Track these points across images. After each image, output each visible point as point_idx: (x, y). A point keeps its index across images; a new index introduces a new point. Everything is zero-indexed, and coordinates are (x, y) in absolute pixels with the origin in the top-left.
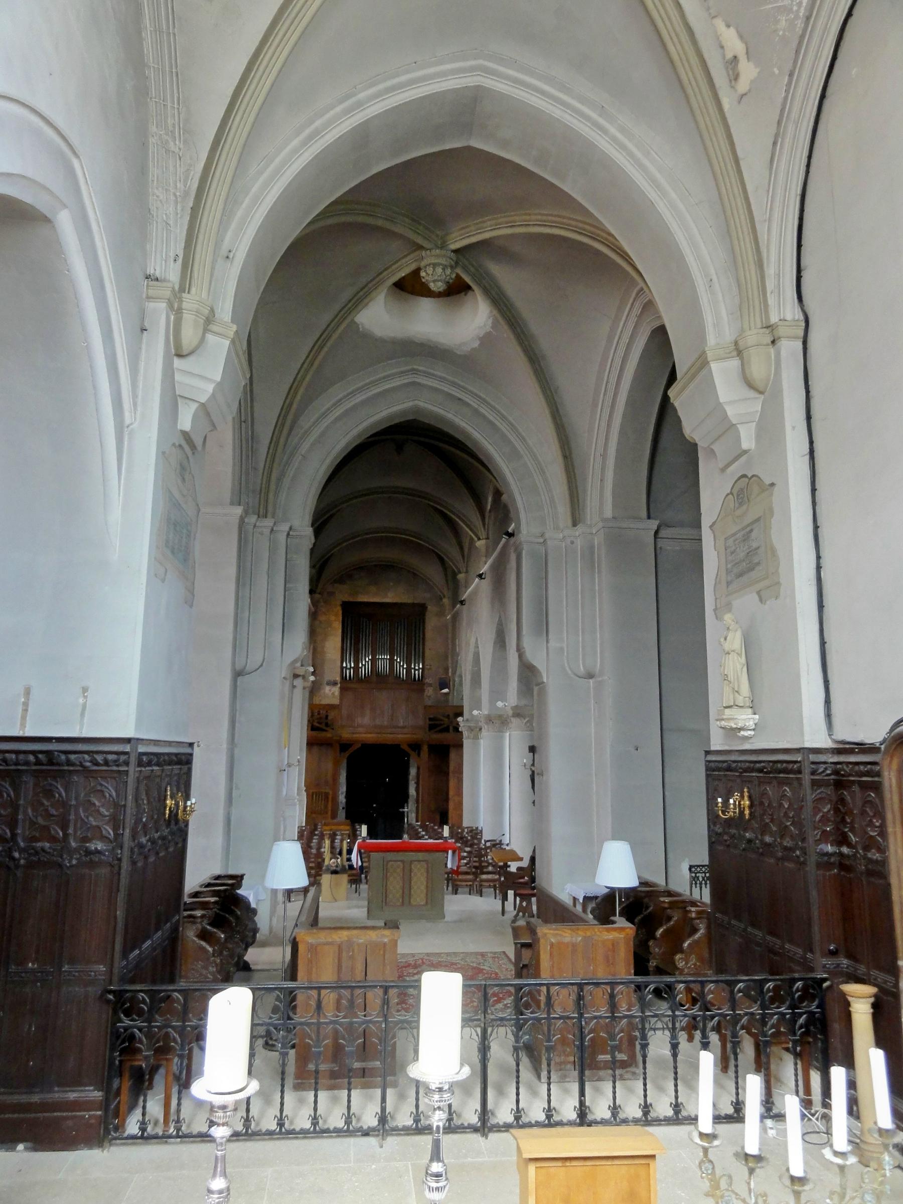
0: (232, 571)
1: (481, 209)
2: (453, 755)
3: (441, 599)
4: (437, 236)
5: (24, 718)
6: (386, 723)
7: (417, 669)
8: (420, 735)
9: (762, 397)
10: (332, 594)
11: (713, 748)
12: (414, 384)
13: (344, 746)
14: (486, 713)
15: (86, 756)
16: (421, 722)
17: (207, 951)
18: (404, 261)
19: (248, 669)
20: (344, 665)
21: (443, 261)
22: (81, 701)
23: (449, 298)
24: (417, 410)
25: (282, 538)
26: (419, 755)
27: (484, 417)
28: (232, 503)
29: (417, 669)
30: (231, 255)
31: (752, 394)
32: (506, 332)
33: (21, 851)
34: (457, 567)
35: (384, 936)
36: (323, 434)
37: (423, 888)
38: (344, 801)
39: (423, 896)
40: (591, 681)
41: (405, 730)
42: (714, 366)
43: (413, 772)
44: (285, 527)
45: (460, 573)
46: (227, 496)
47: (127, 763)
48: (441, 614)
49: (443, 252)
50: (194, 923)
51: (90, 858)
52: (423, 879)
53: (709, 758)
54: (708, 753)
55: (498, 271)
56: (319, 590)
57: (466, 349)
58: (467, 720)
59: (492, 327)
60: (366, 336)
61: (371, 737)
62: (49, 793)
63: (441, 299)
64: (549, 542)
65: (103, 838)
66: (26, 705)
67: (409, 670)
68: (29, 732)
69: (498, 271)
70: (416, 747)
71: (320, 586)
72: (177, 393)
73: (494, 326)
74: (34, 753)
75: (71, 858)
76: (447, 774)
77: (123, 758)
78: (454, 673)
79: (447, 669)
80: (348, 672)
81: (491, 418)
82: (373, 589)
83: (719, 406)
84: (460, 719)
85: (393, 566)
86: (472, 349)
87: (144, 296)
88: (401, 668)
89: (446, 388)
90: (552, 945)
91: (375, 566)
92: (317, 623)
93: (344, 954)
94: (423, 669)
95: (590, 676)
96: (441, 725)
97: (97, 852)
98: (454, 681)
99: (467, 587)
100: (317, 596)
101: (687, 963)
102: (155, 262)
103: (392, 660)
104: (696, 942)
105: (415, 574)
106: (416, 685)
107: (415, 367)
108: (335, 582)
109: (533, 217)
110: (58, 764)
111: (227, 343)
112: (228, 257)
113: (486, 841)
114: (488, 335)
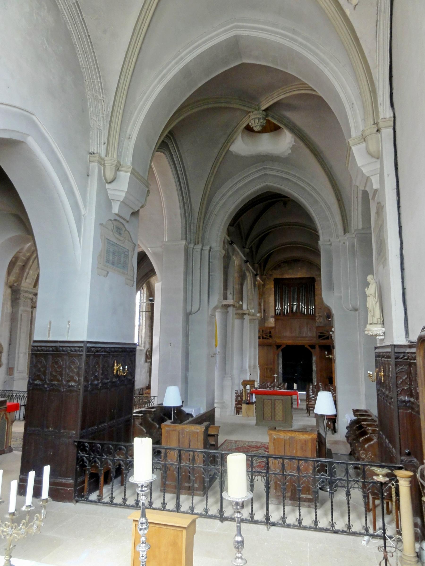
0: (182, 269)
1: (270, 89)
4: (256, 105)
5: (49, 333)
6: (297, 335)
7: (311, 309)
8: (315, 341)
9: (379, 160)
10: (271, 275)
11: (378, 345)
12: (265, 175)
13: (278, 347)
15: (69, 348)
16: (314, 335)
17: (143, 431)
18: (244, 119)
19: (193, 311)
21: (259, 116)
22: (68, 326)
23: (275, 132)
24: (267, 186)
25: (207, 253)
27: (299, 185)
28: (182, 240)
29: (311, 309)
30: (131, 137)
31: (374, 160)
32: (302, 144)
33: (48, 384)
35: (198, 429)
36: (224, 204)
37: (281, 412)
38: (281, 372)
39: (281, 416)
40: (357, 312)
41: (307, 339)
42: (353, 148)
43: (314, 359)
44: (208, 248)
46: (180, 236)
47: (82, 351)
49: (258, 112)
50: (139, 419)
51: (70, 390)
52: (281, 408)
53: (377, 350)
54: (376, 348)
55: (288, 114)
57: (286, 154)
59: (295, 142)
60: (238, 157)
61: (290, 342)
62: (56, 363)
63: (273, 132)
64: (333, 244)
65: (75, 381)
66: (50, 328)
67: (307, 309)
68: (51, 339)
69: (288, 114)
71: (265, 272)
72: (110, 198)
73: (295, 141)
74: (52, 347)
75: (63, 389)
77: (81, 349)
80: (278, 311)
81: (303, 186)
82: (290, 271)
83: (358, 168)
86: (288, 154)
87: (89, 161)
88: (303, 308)
89: (279, 174)
90: (275, 439)
92: (265, 289)
93: (181, 436)
94: (315, 309)
95: (356, 310)
96: (324, 336)
97: (72, 386)
100: (264, 277)
101: (366, 456)
102: (94, 147)
103: (299, 305)
104: (371, 446)
105: (311, 263)
106: (312, 317)
107: (265, 167)
108: (272, 270)
109: (293, 87)
110: (59, 351)
111: (129, 174)
112: (129, 138)
114: (293, 145)
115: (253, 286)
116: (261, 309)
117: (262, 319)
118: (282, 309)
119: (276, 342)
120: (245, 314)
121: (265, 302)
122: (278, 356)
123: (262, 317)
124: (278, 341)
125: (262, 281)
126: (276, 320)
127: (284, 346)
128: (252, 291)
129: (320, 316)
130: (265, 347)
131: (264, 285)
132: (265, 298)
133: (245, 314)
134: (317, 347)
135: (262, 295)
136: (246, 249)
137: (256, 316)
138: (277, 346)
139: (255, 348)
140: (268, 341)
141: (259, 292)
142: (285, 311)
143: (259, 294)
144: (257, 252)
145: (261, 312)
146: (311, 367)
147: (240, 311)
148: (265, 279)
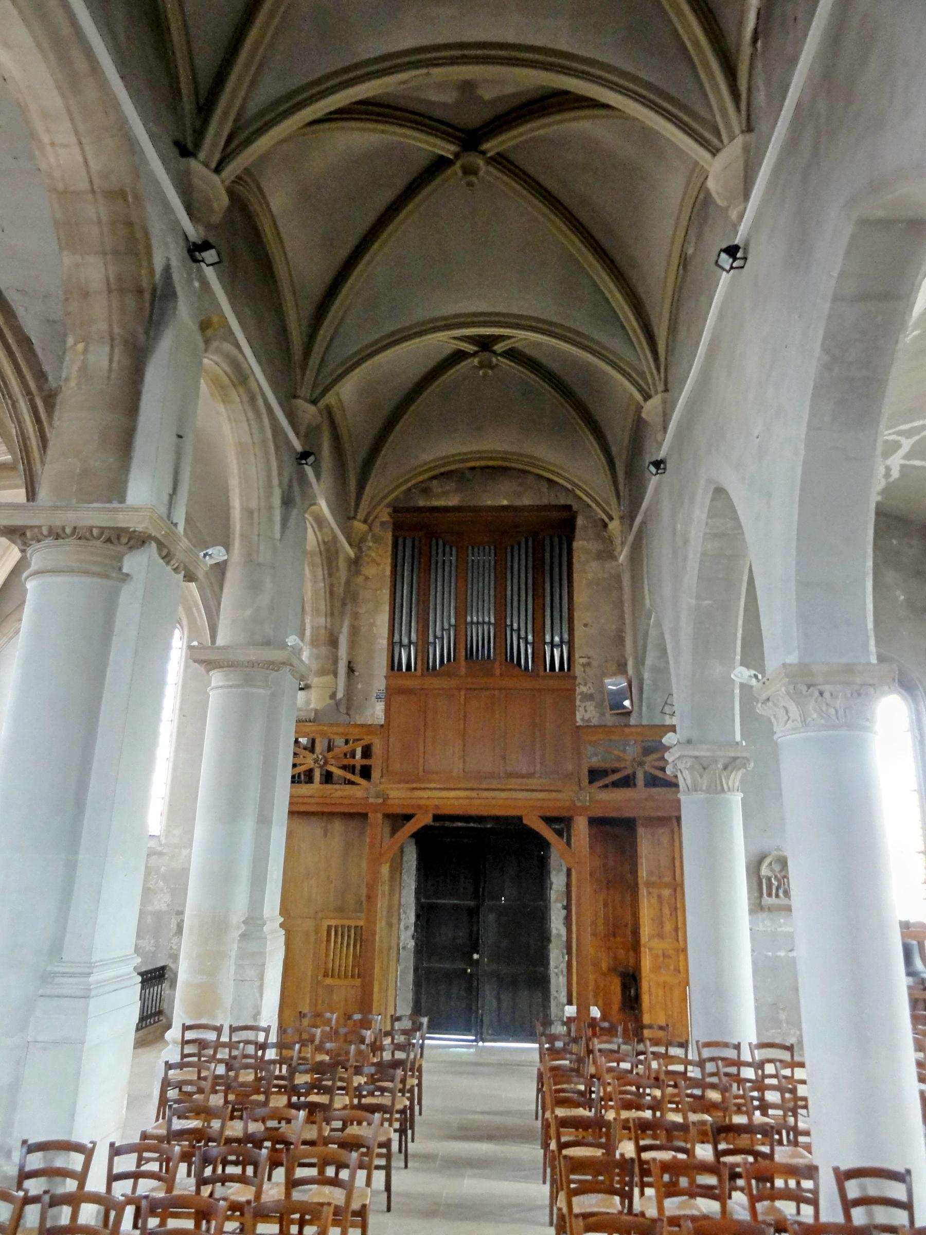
2: (647, 847)
3: (605, 526)
6: (487, 767)
13: (398, 820)
14: (793, 659)
20: (397, 638)
26: (569, 843)
34: (641, 390)
38: (412, 944)
41: (533, 783)
43: (557, 881)
45: (647, 397)
48: (607, 554)
56: (361, 515)
58: (689, 742)
61: (454, 799)
70: (561, 823)
71: (364, 505)
76: (634, 888)
78: (640, 662)
79: (621, 668)
84: (669, 739)
85: (504, 470)
91: (473, 469)
92: (360, 580)
98: (641, 681)
99: (665, 429)
103: (501, 625)
113: (843, 1176)
115: (277, 500)
116: (335, 661)
117: (337, 705)
118: (424, 645)
119: (386, 798)
120: (138, 540)
121: (354, 632)
122: (397, 868)
123: (340, 695)
124: (398, 795)
125: (351, 545)
126: (391, 694)
127: (425, 820)
128: (271, 520)
129: (588, 697)
130: (338, 826)
131: (355, 564)
132: (356, 616)
133: (138, 540)
134: (581, 826)
135: (342, 599)
136: (194, 165)
137: (284, 646)
138: (387, 816)
139: (264, 820)
140: (349, 790)
141: (332, 585)
142: (436, 653)
143: (332, 593)
144: (307, 353)
145: (335, 674)
146: (541, 917)
147: (95, 516)
148: (363, 540)
